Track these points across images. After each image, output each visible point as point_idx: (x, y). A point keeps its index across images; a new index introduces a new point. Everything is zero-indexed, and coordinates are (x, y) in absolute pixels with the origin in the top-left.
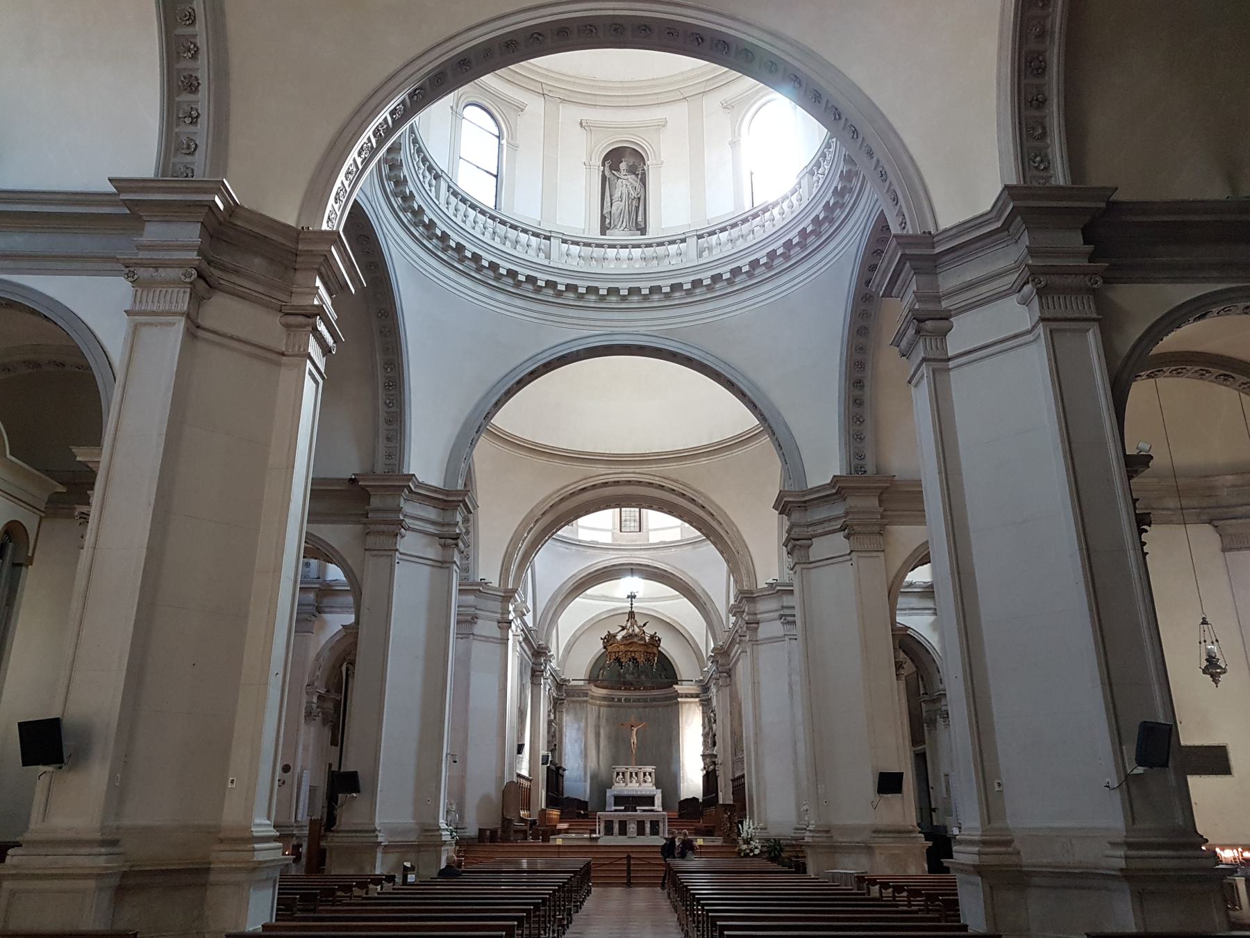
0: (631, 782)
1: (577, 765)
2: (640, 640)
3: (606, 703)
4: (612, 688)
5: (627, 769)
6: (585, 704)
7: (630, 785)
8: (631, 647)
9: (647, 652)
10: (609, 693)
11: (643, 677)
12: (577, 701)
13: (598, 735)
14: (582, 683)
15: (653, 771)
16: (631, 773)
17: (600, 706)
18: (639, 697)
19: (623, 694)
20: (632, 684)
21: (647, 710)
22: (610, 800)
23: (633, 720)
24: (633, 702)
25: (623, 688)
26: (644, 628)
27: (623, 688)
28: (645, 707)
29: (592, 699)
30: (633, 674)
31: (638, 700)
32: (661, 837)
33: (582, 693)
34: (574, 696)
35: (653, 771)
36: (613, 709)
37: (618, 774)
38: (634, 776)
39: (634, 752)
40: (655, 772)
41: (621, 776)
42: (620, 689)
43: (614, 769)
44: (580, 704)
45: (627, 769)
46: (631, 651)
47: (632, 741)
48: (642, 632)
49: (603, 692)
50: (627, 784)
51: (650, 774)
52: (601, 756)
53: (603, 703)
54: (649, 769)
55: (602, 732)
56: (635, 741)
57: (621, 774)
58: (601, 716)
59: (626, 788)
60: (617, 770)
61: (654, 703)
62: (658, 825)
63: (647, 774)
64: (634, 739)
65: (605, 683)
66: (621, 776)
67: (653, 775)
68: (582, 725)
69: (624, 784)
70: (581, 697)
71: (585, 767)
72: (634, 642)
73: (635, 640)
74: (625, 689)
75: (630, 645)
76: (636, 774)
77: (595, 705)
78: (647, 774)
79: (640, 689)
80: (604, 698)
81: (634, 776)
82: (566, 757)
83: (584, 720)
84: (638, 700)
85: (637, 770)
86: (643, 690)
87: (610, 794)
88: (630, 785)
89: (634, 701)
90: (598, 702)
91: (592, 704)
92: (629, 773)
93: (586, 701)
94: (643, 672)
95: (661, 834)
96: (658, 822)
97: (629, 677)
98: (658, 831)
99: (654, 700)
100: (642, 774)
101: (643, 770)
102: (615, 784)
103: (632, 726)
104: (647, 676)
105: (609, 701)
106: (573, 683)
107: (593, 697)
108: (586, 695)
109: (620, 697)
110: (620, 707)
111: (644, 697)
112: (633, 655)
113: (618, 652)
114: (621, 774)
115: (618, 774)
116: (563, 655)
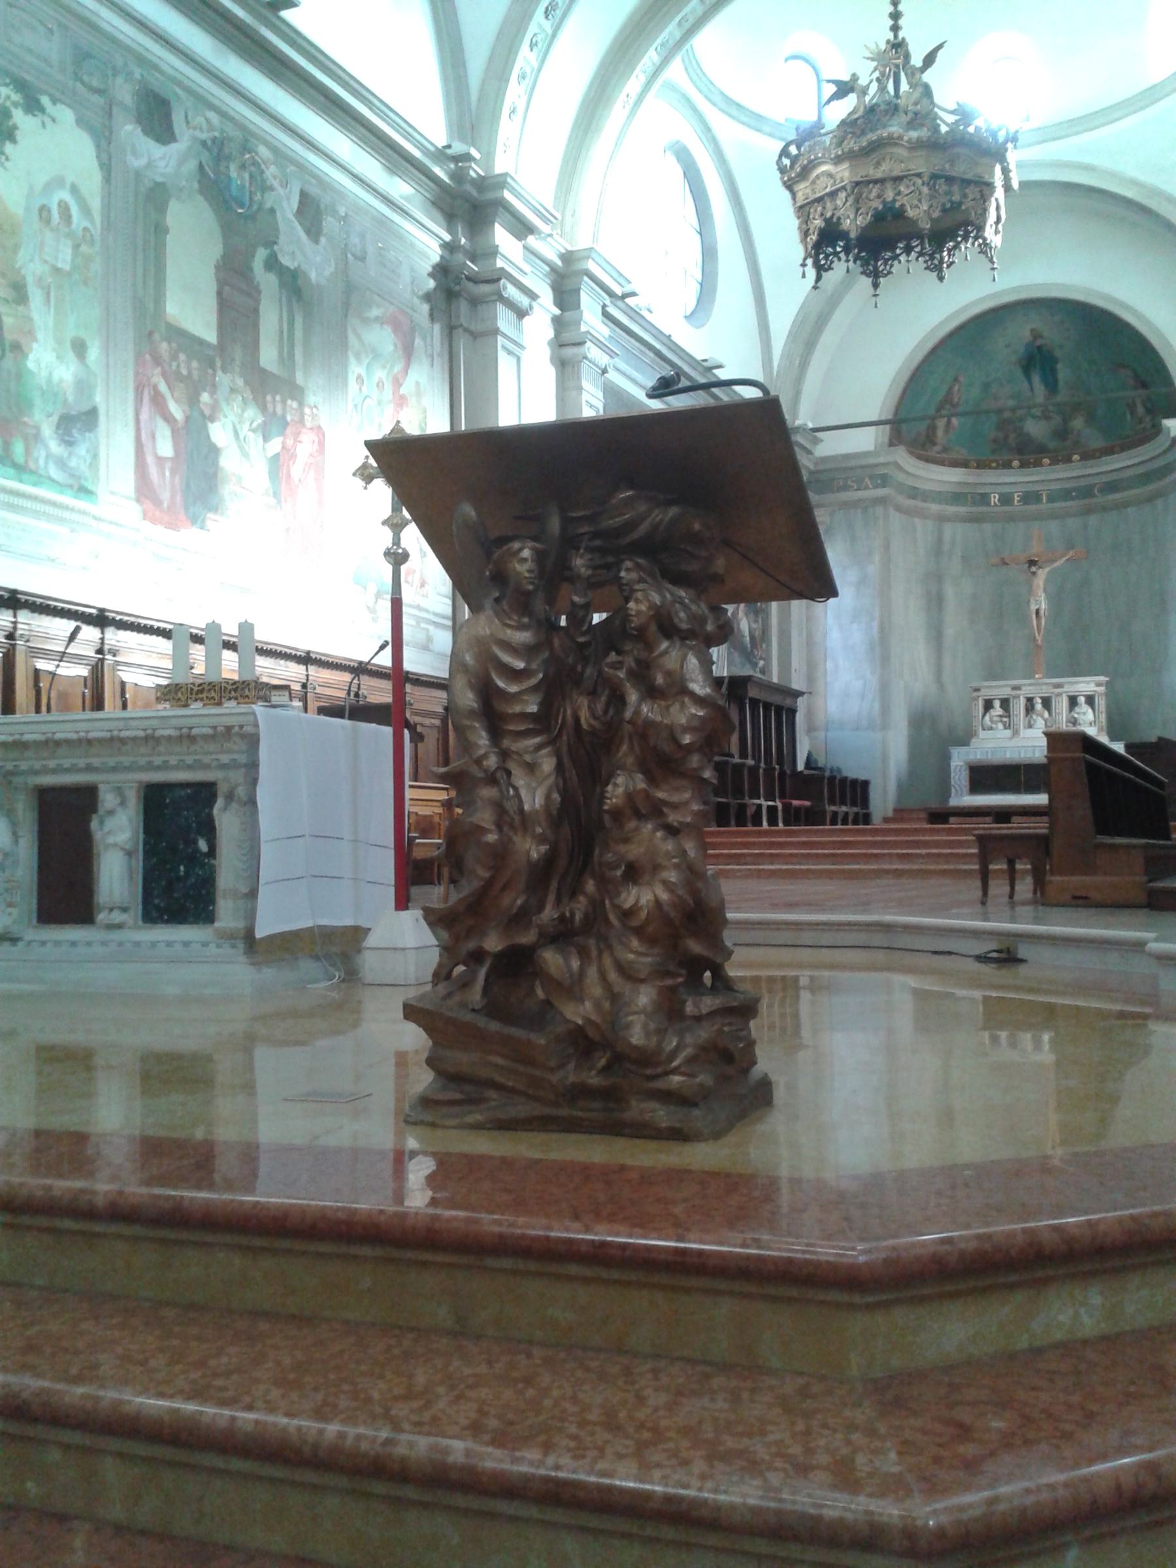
0: (1030, 726)
1: (861, 682)
2: (911, 125)
3: (962, 510)
4: (982, 465)
6: (879, 510)
7: (1025, 733)
8: (878, 164)
9: (950, 180)
10: (971, 479)
11: (1078, 423)
12: (855, 504)
13: (935, 603)
14: (864, 441)
15: (1102, 689)
16: (1030, 701)
17: (942, 519)
18: (1068, 485)
19: (1016, 479)
20: (1042, 450)
21: (1093, 520)
22: (959, 776)
23: (1035, 549)
24: (1051, 499)
25: (1016, 463)
26: (927, 77)
27: (1016, 463)
28: (1089, 511)
29: (913, 497)
30: (1046, 417)
31: (1066, 495)
32: (228, 936)
33: (871, 478)
34: (846, 488)
35: (1102, 689)
36: (988, 527)
37: (988, 705)
38: (1039, 706)
39: (1039, 639)
40: (1107, 695)
41: (997, 710)
42: (1007, 465)
43: (977, 690)
44: (865, 510)
46: (882, 181)
47: (1033, 607)
48: (920, 90)
49: (951, 477)
50: (1016, 733)
51: (1090, 700)
52: (947, 660)
53: (951, 509)
54: (1086, 685)
55: (949, 591)
56: (1043, 606)
57: (997, 704)
58: (946, 547)
59: (1015, 742)
60: (987, 693)
61: (1112, 497)
62: (209, 829)
63: (1082, 700)
64: (1041, 602)
65: (963, 453)
66: (997, 710)
67: (1101, 703)
68: (873, 569)
69: (1008, 733)
70: (866, 488)
71: (884, 689)
72: (892, 141)
73: (894, 128)
74: (1023, 465)
75: (874, 157)
76: (1047, 703)
77: (922, 514)
78: (1082, 700)
79: (1069, 460)
80: (957, 498)
81: (1039, 706)
82: (829, 665)
83: (877, 558)
84: (1066, 495)
85: (1046, 691)
86: (1081, 459)
87: (960, 759)
88: (1025, 733)
89: (1051, 499)
90: (934, 508)
91: (898, 509)
92: (1022, 701)
93: (882, 501)
94: (1076, 408)
95: (227, 913)
96: (205, 793)
97: (1036, 429)
98: (209, 882)
99: (1112, 487)
100: (1065, 702)
101: (1065, 689)
102: (982, 734)
103: (1032, 563)
104: (1091, 418)
105: (974, 504)
106: (831, 446)
107: (914, 493)
108: (884, 480)
109: (1007, 489)
110: (1011, 518)
111: (1083, 483)
112: (889, 195)
113: (833, 194)
114: (997, 704)
115: (988, 705)
116: (787, 355)
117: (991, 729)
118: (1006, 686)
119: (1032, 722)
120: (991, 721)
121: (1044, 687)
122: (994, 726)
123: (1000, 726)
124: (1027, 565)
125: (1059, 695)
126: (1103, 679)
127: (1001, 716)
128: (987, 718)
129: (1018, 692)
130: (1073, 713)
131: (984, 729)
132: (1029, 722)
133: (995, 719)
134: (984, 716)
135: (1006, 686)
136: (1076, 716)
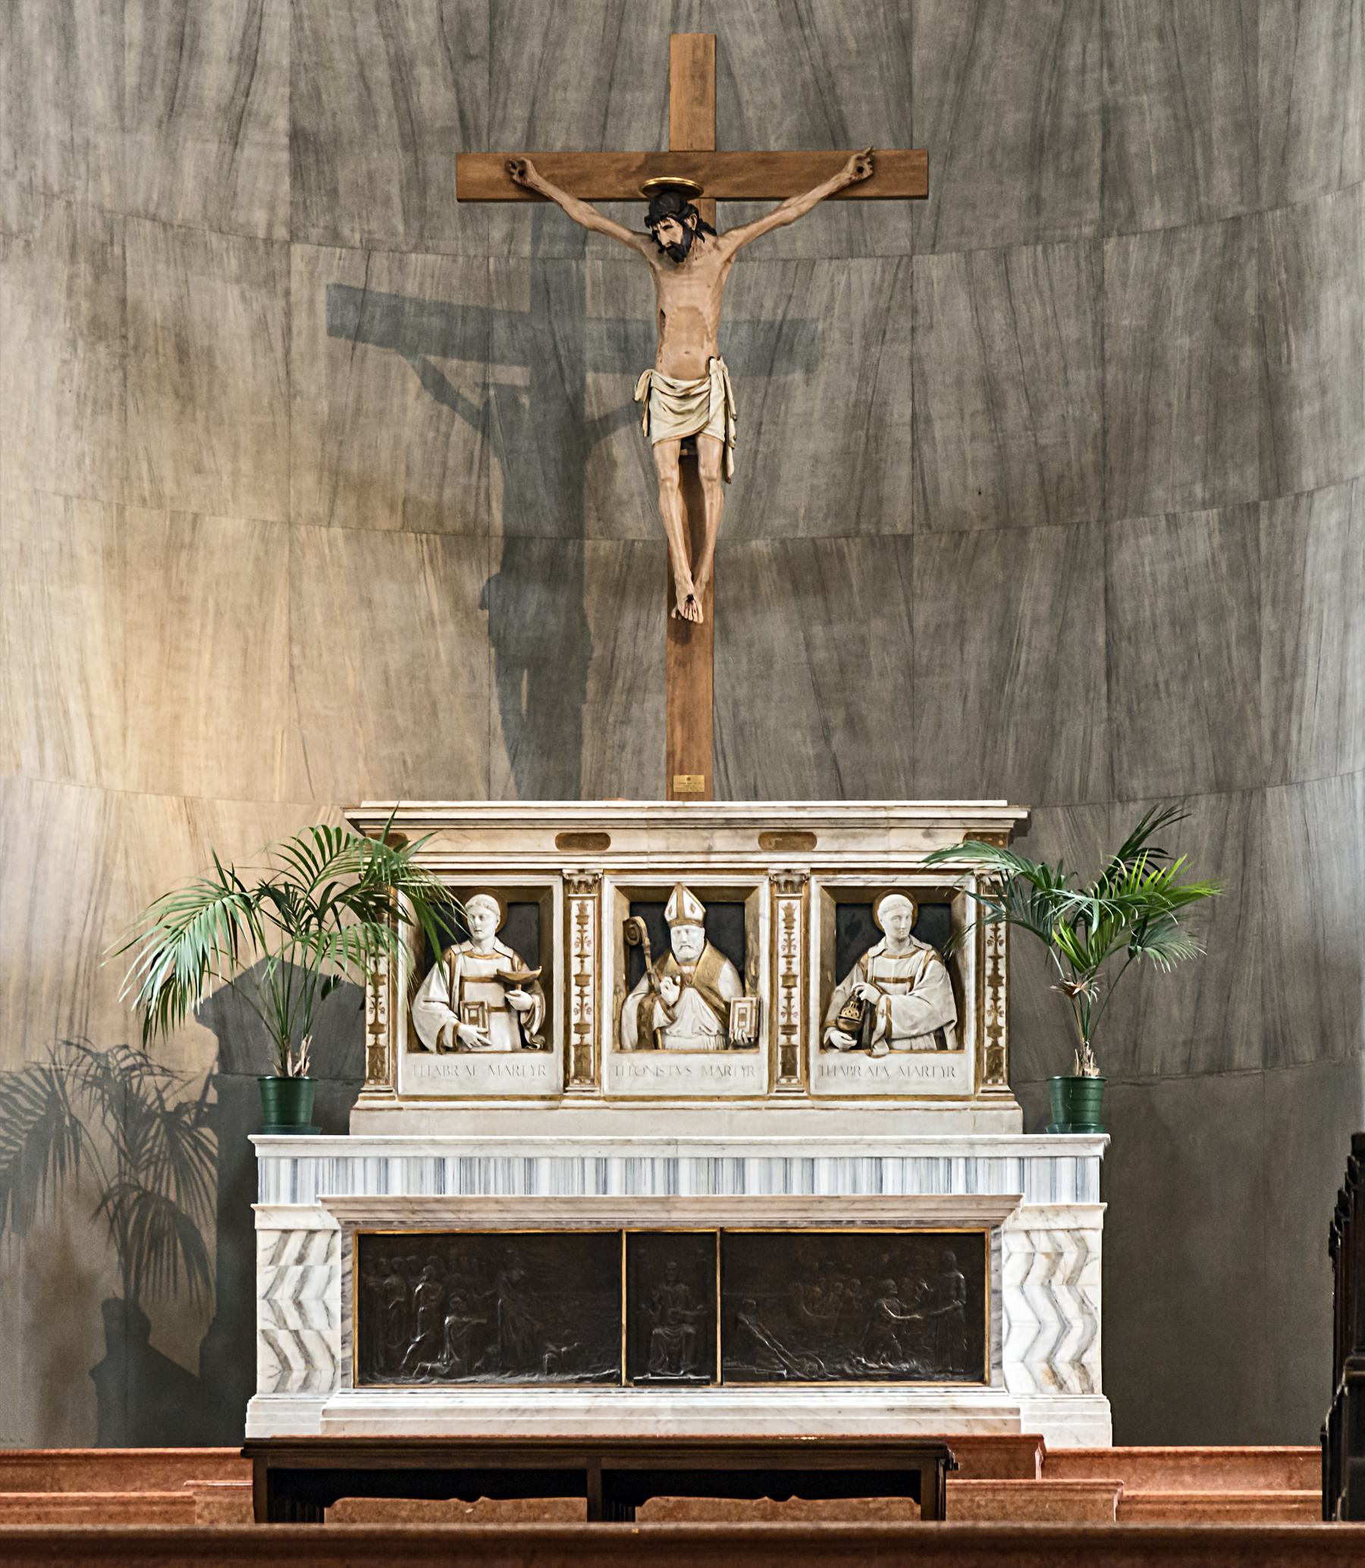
5: (594, 839)
45: (594, 839)
57: (485, 914)
92: (613, 908)
101: (828, 851)
114: (485, 914)
117: (459, 1045)
118: (531, 824)
119: (659, 1018)
120: (457, 1004)
121: (722, 840)
122: (468, 1031)
123: (502, 1031)
124: (643, 209)
125: (790, 884)
126: (1002, 811)
127: (501, 980)
128: (435, 986)
129: (593, 861)
130: (855, 981)
131: (417, 1046)
132: (644, 1017)
133: (473, 992)
134: (421, 971)
135: (531, 824)
136: (869, 993)
